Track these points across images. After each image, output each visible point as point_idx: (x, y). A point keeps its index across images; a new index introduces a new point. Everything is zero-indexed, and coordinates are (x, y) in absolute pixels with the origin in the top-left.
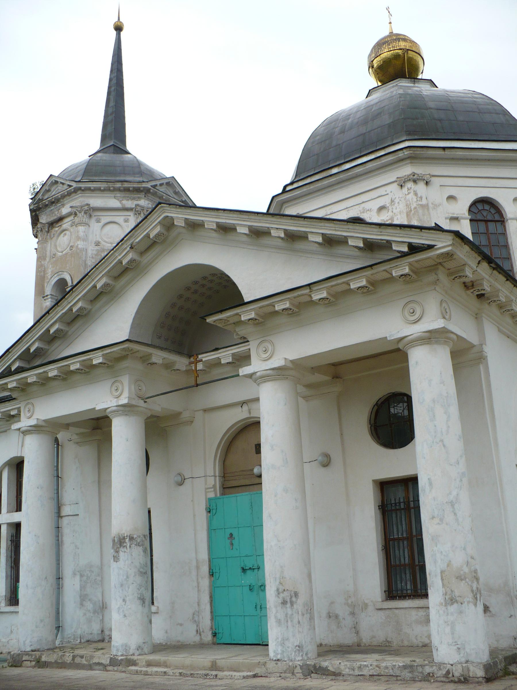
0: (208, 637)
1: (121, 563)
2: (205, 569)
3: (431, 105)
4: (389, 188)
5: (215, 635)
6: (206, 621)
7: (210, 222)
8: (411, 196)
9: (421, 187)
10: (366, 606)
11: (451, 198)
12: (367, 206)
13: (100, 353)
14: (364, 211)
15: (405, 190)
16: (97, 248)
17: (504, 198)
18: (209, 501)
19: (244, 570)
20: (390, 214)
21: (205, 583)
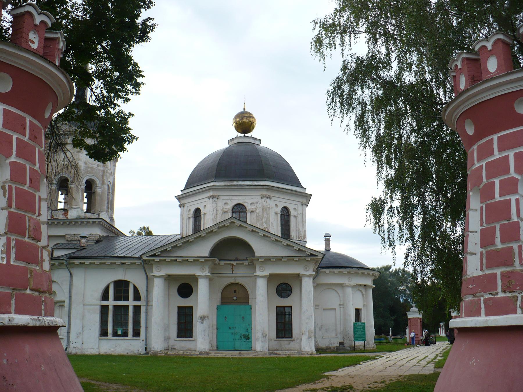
0: (215, 348)
1: (204, 324)
2: (215, 327)
3: (271, 163)
4: (257, 197)
5: (217, 348)
6: (215, 343)
7: (251, 228)
8: (265, 203)
9: (268, 200)
10: (271, 340)
11: (276, 205)
12: (247, 201)
13: (204, 259)
14: (245, 202)
15: (263, 200)
16: (86, 165)
17: (291, 208)
18: (217, 306)
19: (230, 328)
20: (255, 207)
21: (215, 331)
